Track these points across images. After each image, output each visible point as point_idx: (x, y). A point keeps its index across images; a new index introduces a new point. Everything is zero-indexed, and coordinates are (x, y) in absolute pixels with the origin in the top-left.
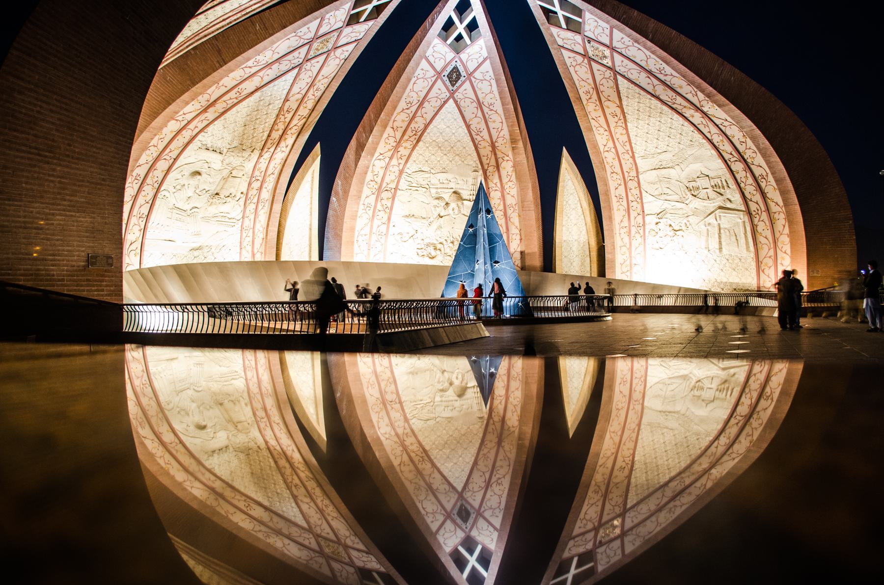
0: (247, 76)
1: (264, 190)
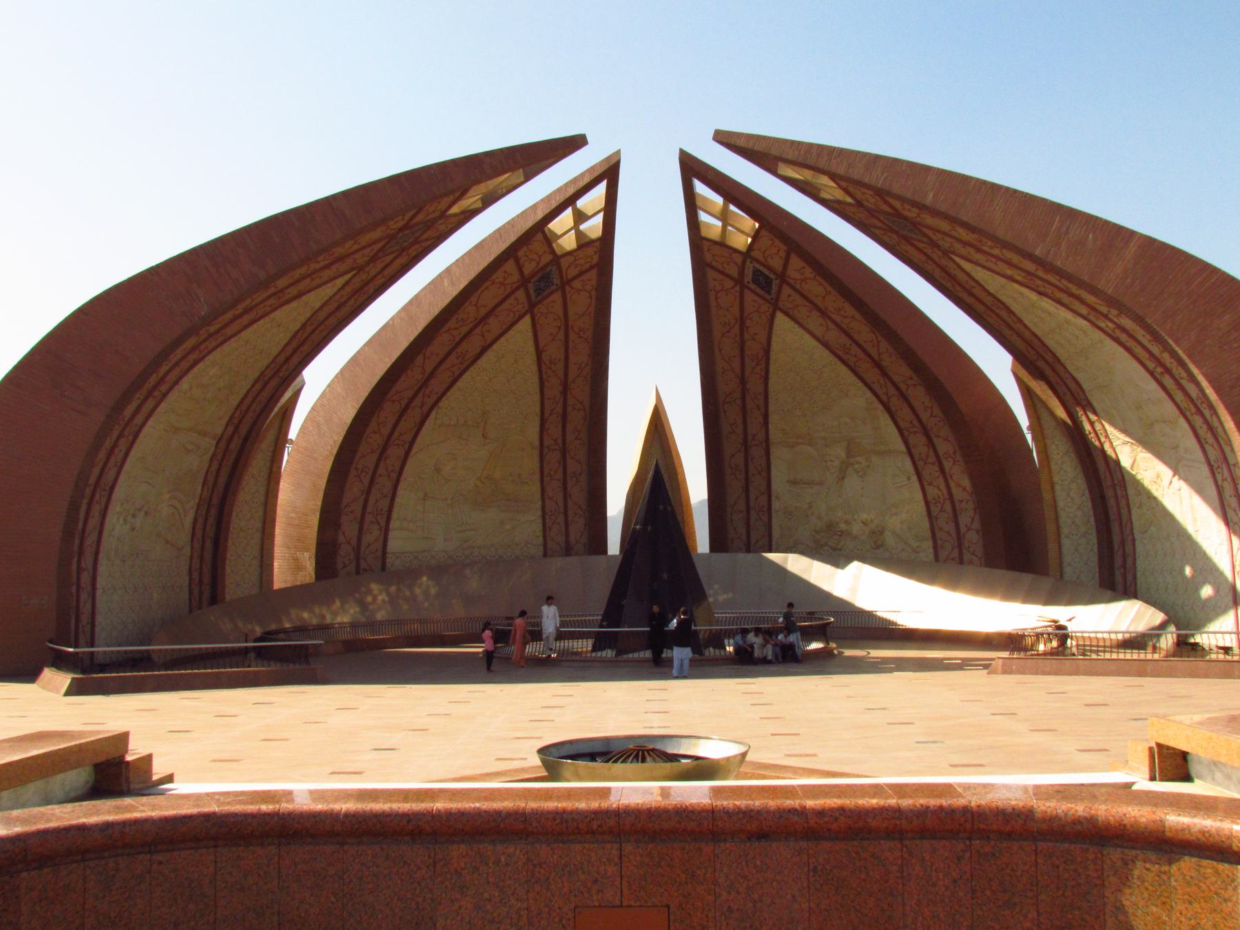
0: (457, 339)
1: (569, 461)
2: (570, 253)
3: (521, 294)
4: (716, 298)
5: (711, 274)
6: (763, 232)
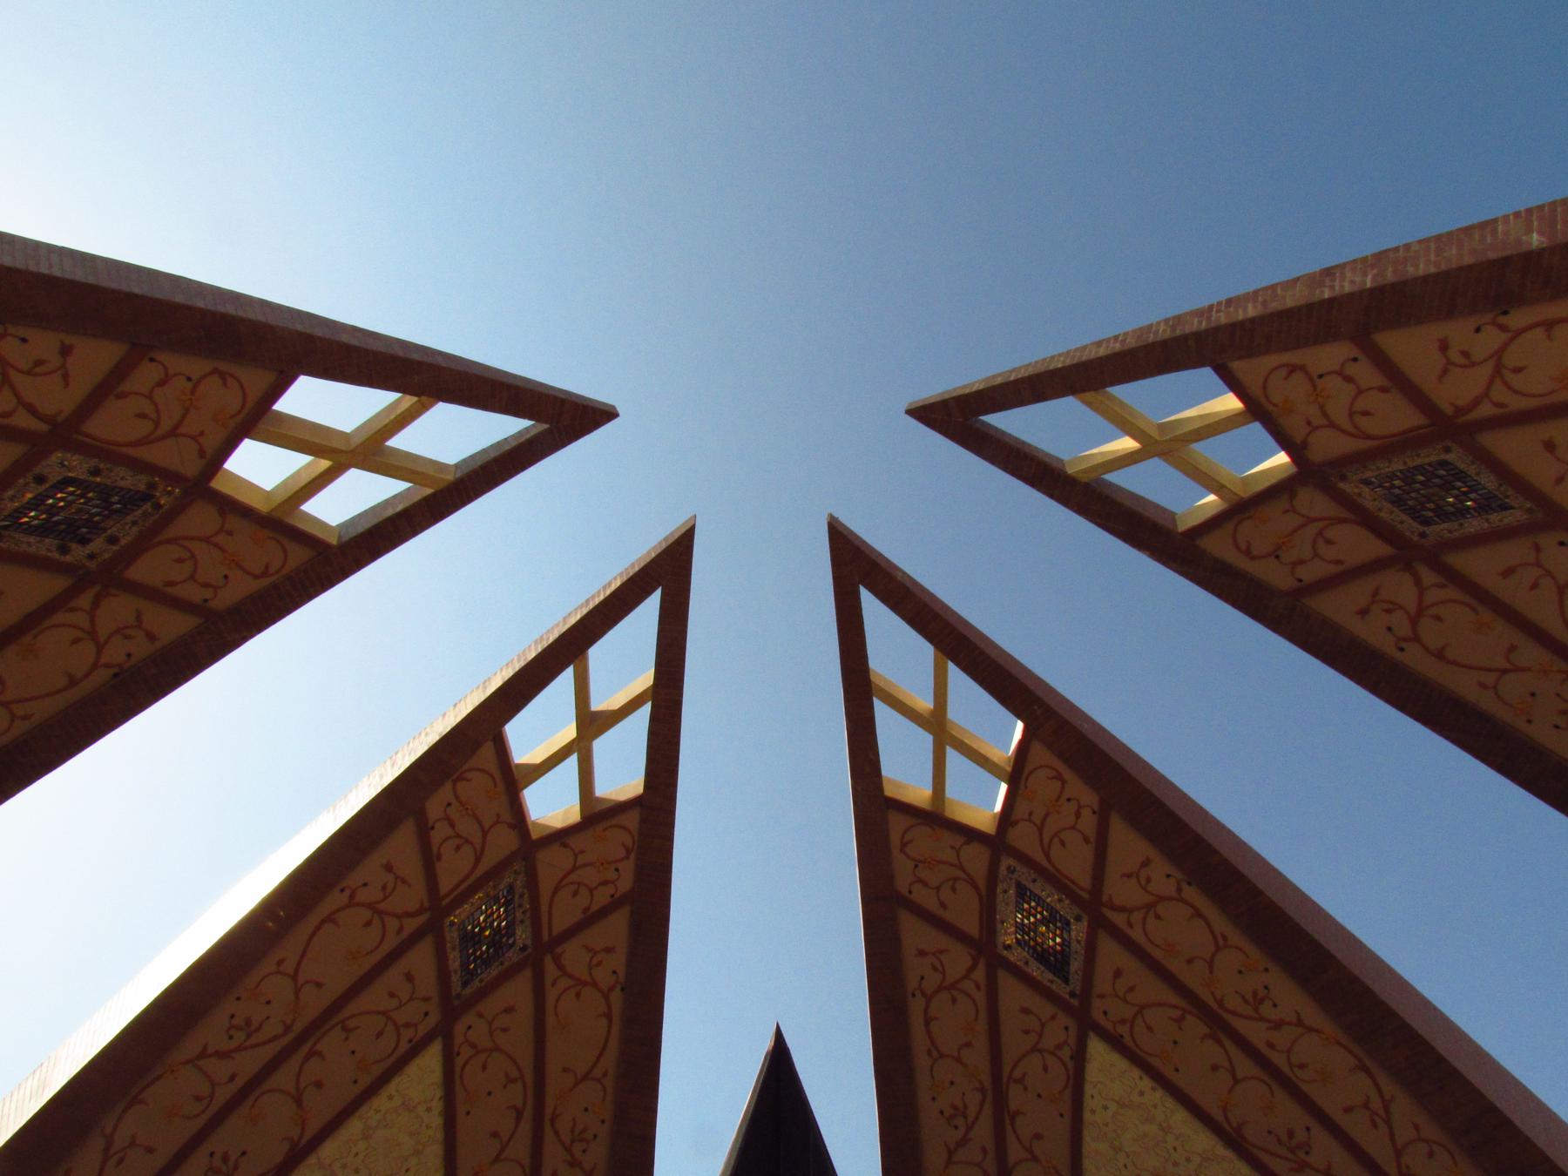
0: (223, 1095)
2: (560, 837)
3: (421, 959)
4: (928, 1021)
5: (915, 934)
6: (1039, 753)
